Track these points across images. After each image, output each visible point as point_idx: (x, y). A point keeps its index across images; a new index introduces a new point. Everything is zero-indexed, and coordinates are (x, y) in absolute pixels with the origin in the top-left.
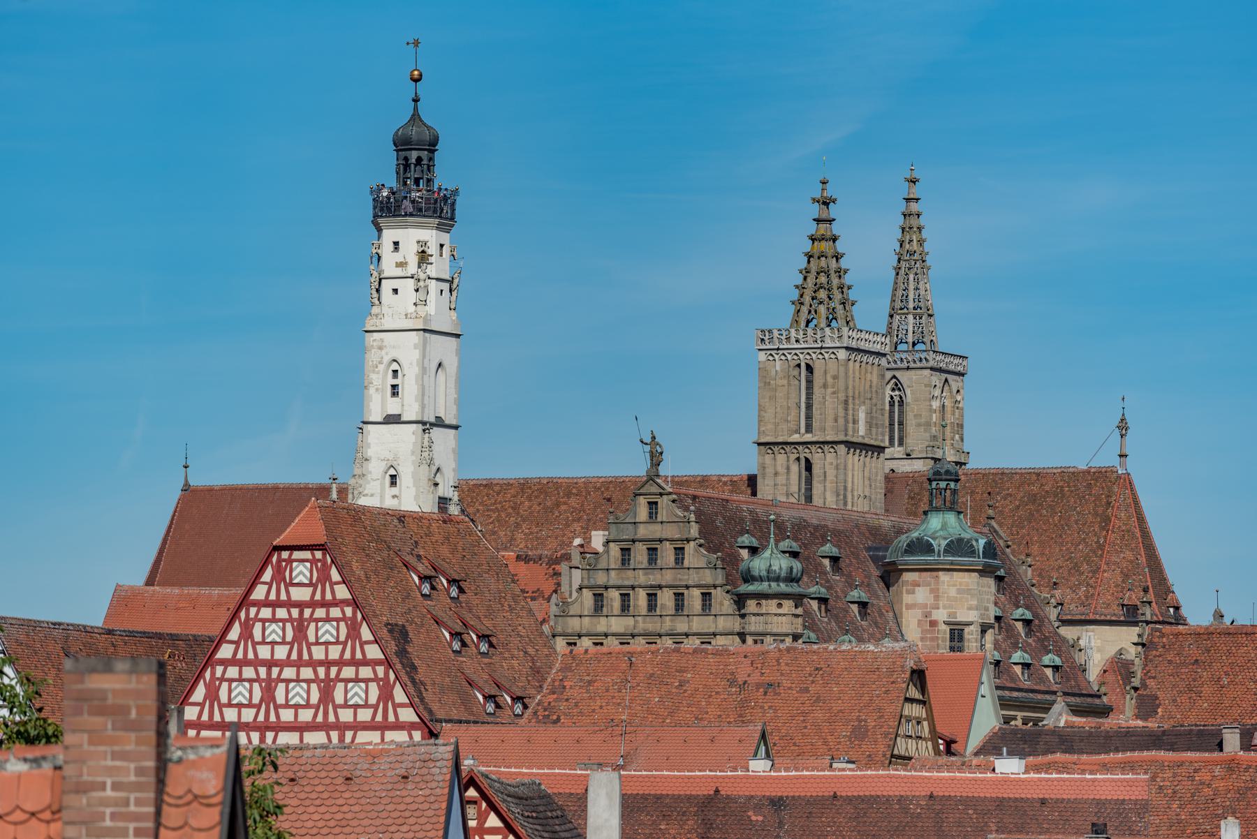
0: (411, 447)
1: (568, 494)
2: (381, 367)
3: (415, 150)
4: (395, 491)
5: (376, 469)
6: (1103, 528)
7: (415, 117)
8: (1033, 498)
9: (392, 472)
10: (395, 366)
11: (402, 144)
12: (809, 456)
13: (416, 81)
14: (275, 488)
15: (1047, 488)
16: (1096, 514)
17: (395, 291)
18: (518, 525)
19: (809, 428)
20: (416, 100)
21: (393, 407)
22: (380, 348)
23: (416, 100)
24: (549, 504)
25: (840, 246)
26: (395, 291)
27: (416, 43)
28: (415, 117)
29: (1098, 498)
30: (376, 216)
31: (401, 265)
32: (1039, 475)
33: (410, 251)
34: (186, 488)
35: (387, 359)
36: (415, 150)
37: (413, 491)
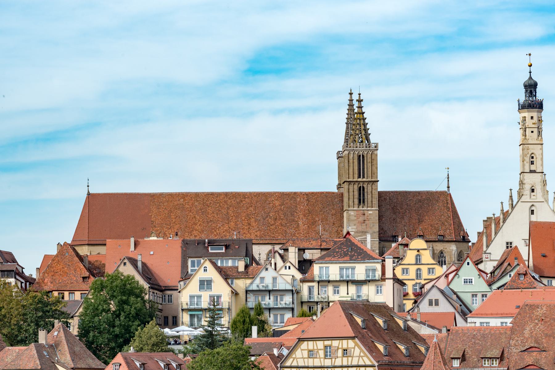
0: (540, 180)
1: (245, 198)
2: (529, 155)
3: (531, 87)
4: (533, 194)
5: (527, 187)
6: (448, 211)
7: (530, 78)
8: (420, 201)
9: (533, 188)
10: (533, 155)
11: (525, 86)
12: (365, 186)
13: (530, 66)
14: (212, 194)
15: (424, 197)
16: (444, 207)
17: (532, 132)
18: (228, 208)
19: (364, 177)
20: (530, 72)
21: (533, 168)
22: (528, 149)
23: (530, 72)
24: (238, 201)
25: (365, 115)
26: (532, 132)
27: (530, 55)
28: (530, 78)
29: (443, 201)
30: (519, 109)
31: (533, 124)
32: (419, 193)
33: (535, 120)
34: (89, 194)
35: (530, 153)
36: (531, 87)
37: (541, 194)
